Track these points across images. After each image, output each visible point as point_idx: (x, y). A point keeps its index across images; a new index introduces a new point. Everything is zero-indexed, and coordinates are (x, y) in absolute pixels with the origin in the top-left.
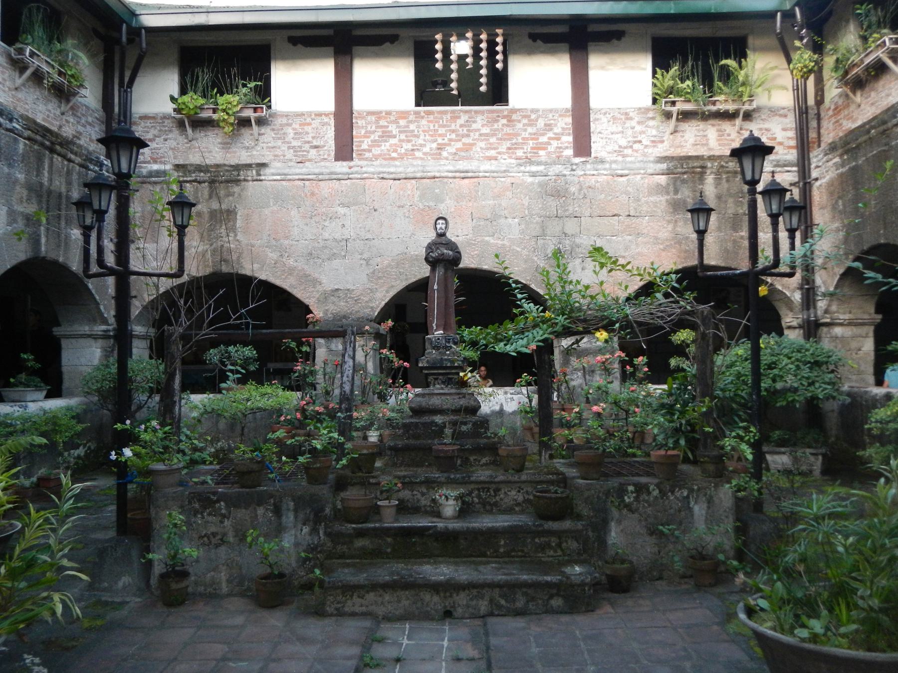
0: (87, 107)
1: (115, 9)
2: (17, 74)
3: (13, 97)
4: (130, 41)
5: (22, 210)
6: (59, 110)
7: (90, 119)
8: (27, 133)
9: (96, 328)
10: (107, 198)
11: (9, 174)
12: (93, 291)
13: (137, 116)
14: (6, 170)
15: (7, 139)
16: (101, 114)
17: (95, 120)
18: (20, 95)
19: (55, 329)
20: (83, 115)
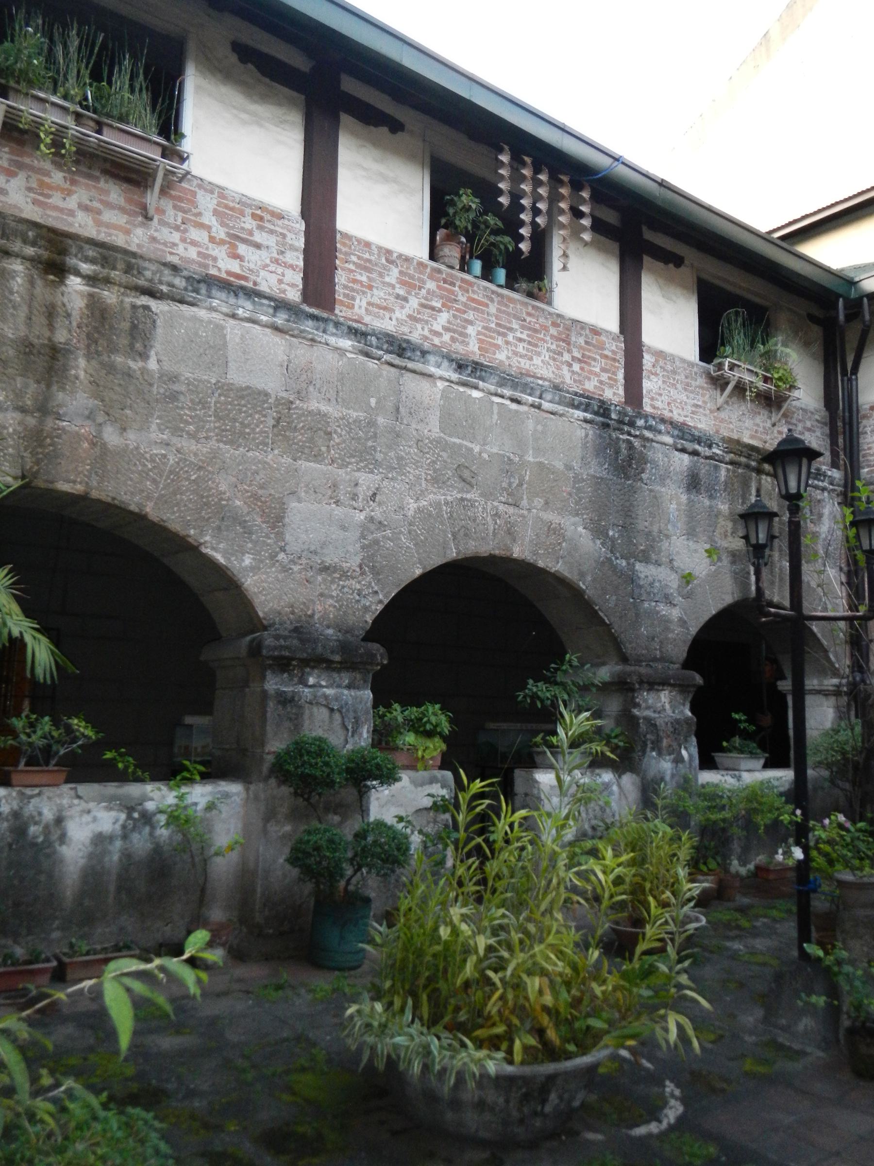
0: (804, 410)
1: (828, 286)
2: (719, 392)
3: (716, 418)
4: (849, 318)
5: (726, 545)
6: (769, 421)
7: (808, 424)
8: (729, 457)
9: (826, 682)
10: (755, 529)
11: (710, 507)
12: (819, 635)
13: (867, 407)
14: (707, 502)
15: (707, 468)
16: (824, 413)
17: (815, 423)
18: (723, 415)
19: (779, 683)
20: (800, 421)
